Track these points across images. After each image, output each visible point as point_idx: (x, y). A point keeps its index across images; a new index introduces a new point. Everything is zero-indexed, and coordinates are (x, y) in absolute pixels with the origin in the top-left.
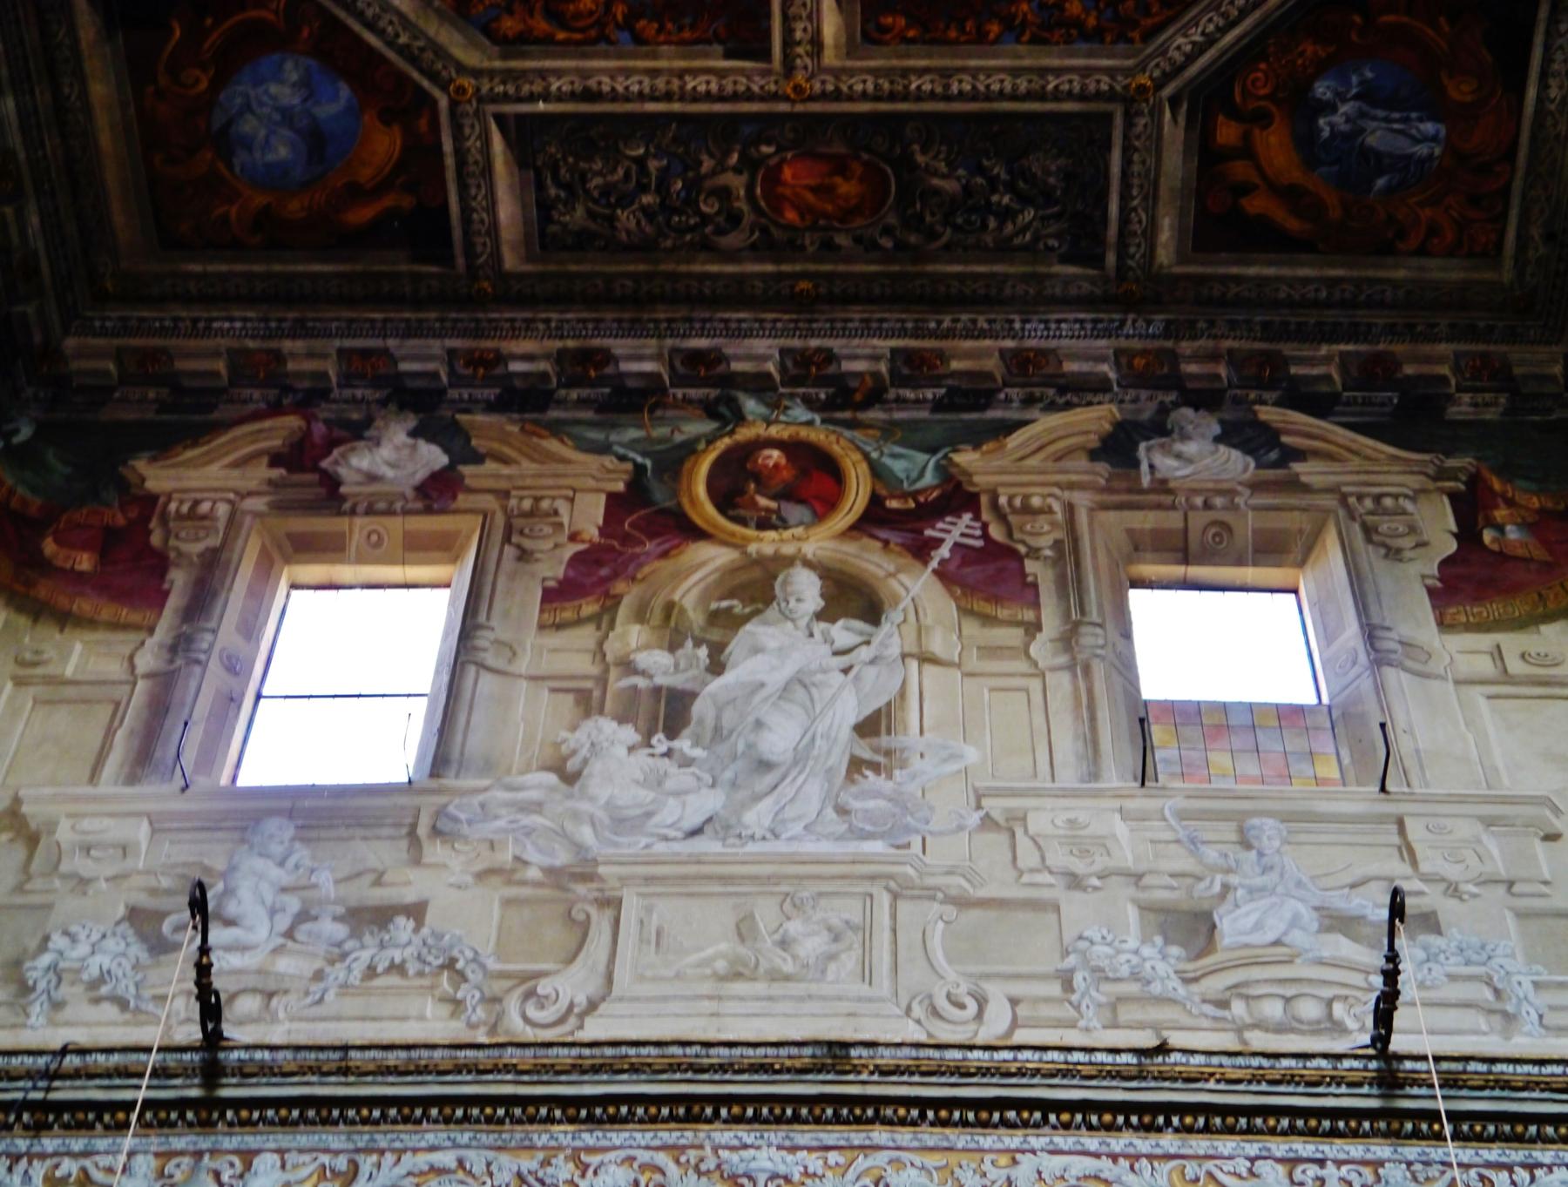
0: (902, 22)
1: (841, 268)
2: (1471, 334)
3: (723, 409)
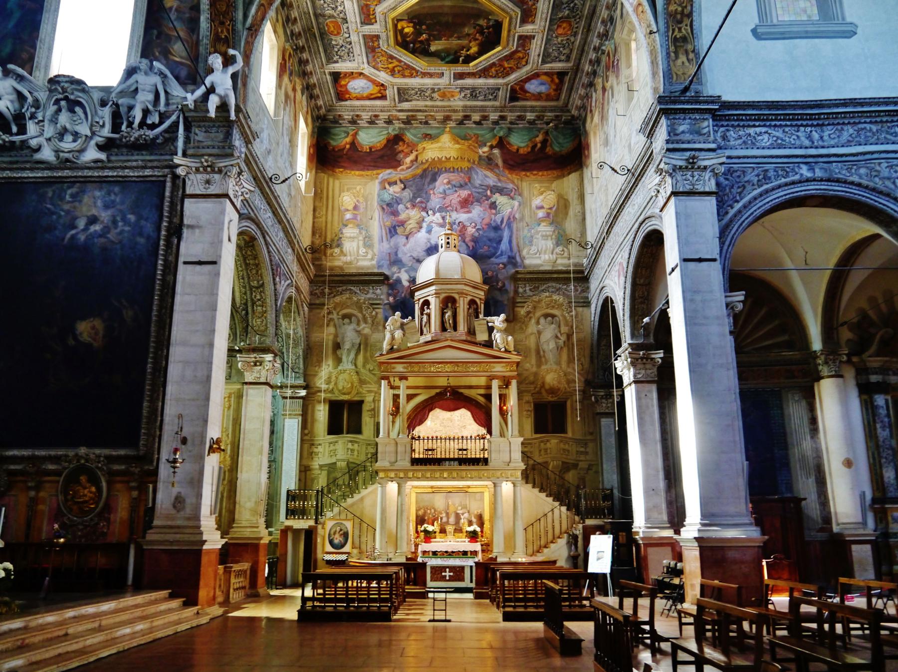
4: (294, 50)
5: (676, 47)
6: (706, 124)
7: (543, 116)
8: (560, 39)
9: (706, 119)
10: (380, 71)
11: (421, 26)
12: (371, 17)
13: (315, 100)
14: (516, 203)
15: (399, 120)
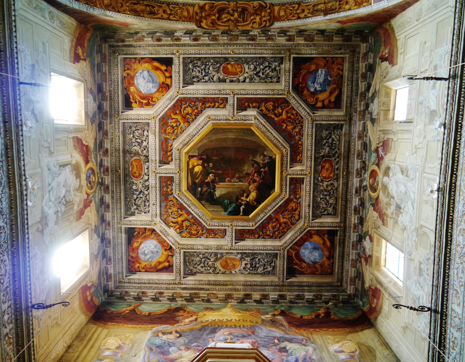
0: (298, 157)
1: (342, 167)
2: (358, 60)
3: (365, 188)
7: (321, 296)
8: (325, 184)
10: (169, 227)
11: (208, 164)
12: (169, 154)
15: (182, 297)
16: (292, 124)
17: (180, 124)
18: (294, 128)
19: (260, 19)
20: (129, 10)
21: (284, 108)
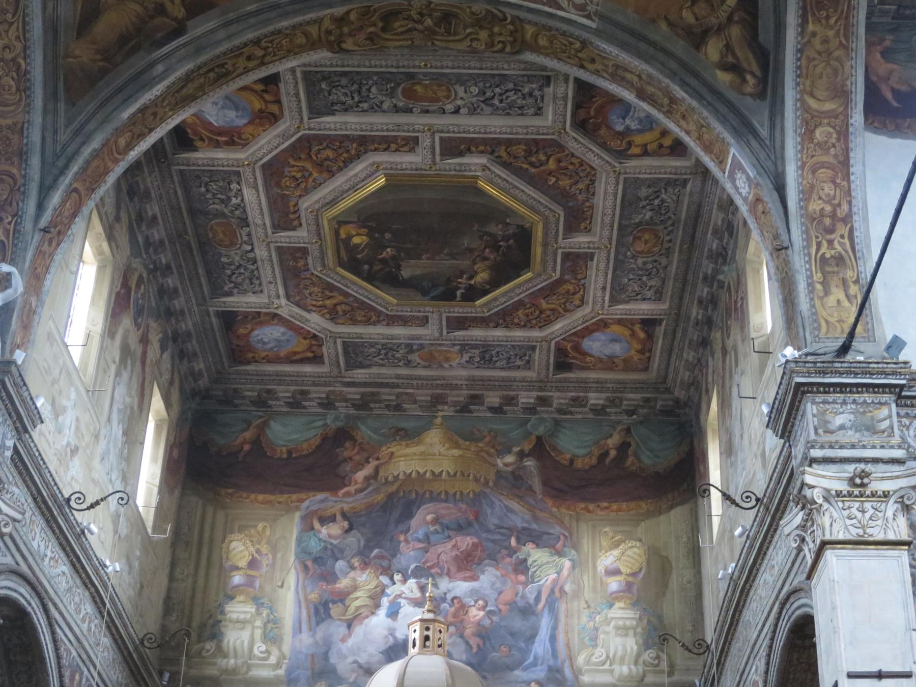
4: (150, 272)
5: (824, 273)
6: (884, 412)
7: (621, 399)
8: (640, 261)
9: (886, 404)
10: (309, 311)
13: (190, 362)
14: (567, 564)
15: (346, 400)
16: (571, 177)
17: (311, 174)
18: (576, 183)
19: (491, 35)
20: (170, 110)
21: (551, 155)
